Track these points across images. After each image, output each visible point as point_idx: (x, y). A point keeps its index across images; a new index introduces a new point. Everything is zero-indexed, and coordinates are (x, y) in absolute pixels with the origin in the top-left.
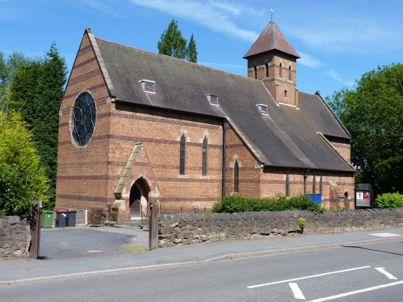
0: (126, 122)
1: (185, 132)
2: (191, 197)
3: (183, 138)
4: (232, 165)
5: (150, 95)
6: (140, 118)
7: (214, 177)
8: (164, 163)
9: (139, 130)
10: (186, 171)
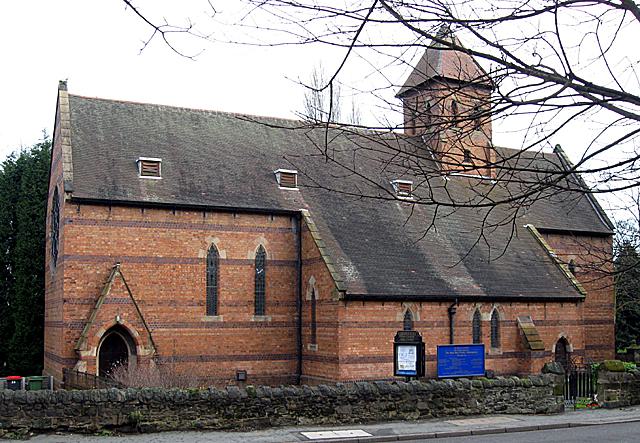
0: (95, 232)
1: (216, 241)
2: (231, 353)
3: (213, 250)
4: (309, 297)
5: (148, 186)
6: (122, 223)
7: (280, 318)
8: (171, 298)
9: (120, 244)
10: (221, 309)
